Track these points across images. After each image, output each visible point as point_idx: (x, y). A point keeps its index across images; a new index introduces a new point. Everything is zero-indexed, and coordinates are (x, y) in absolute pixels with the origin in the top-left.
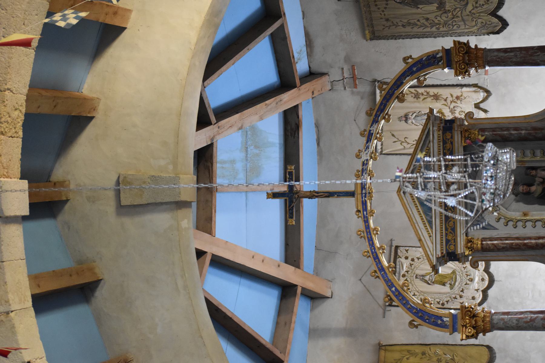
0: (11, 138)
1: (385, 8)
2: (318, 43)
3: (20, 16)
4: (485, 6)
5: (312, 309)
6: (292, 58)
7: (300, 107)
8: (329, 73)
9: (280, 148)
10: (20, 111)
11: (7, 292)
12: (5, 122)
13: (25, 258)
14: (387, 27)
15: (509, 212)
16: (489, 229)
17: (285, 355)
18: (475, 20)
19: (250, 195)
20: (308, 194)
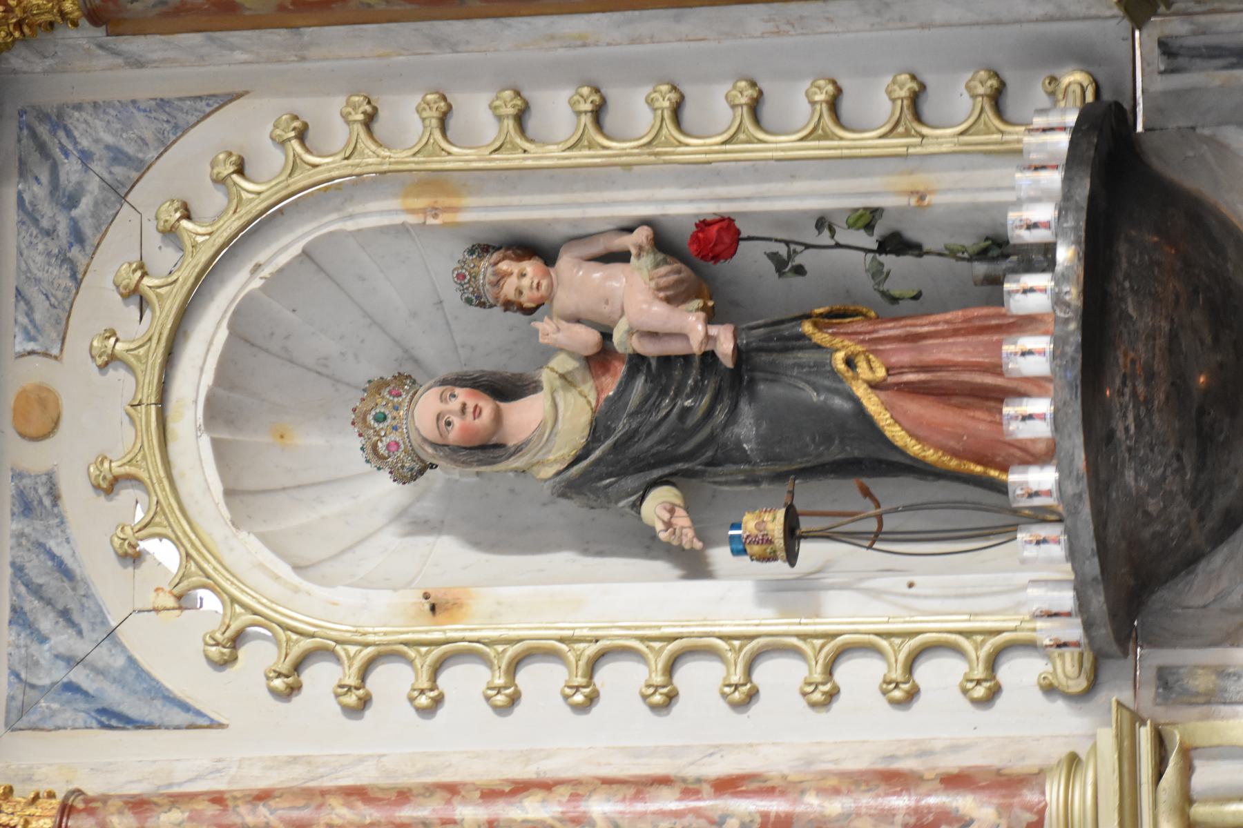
15: (315, 589)
16: (150, 726)
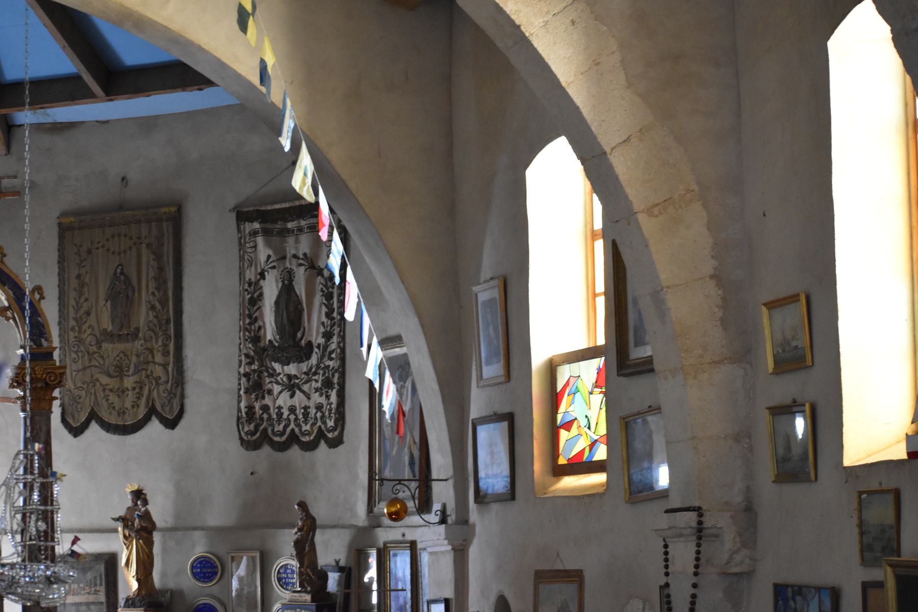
1: (108, 250)
4: (105, 403)
6: (40, 106)
8: (8, 156)
14: (79, 250)
18: (85, 386)
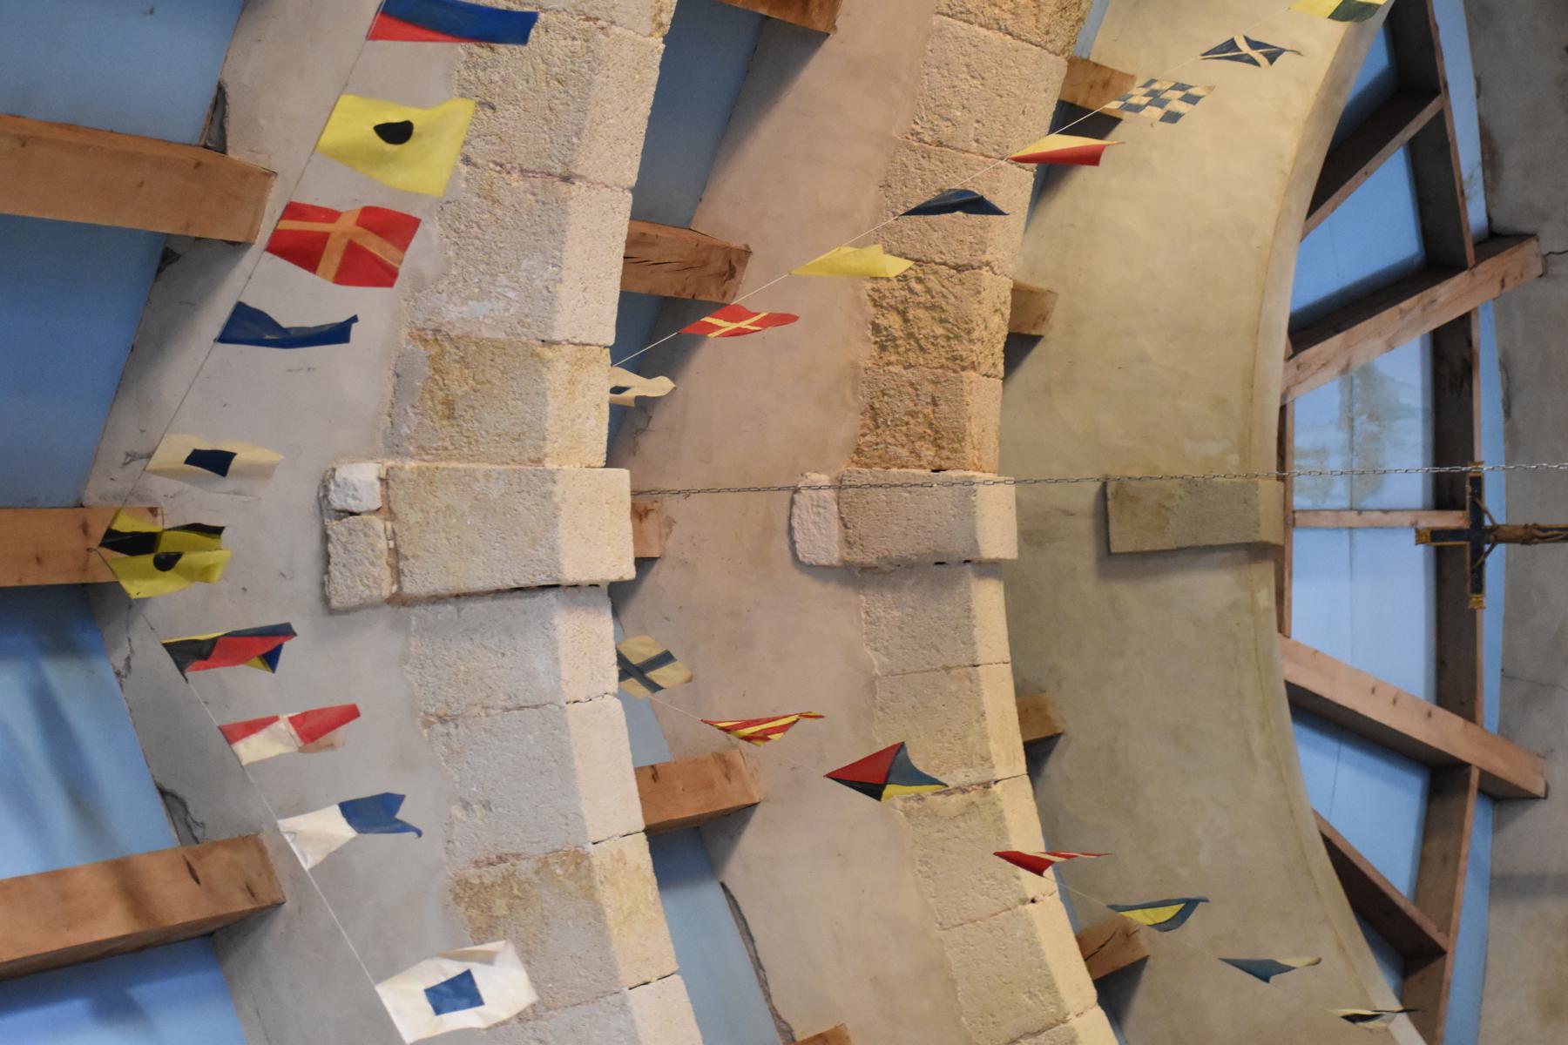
0: (985, 378)
2: (1513, 158)
3: (1018, 93)
5: (1498, 827)
6: (1459, 194)
7: (1473, 317)
8: (1539, 235)
9: (1425, 422)
10: (1002, 314)
11: (986, 737)
12: (979, 340)
13: (1009, 659)
17: (1448, 935)
19: (1360, 536)
20: (1520, 532)
